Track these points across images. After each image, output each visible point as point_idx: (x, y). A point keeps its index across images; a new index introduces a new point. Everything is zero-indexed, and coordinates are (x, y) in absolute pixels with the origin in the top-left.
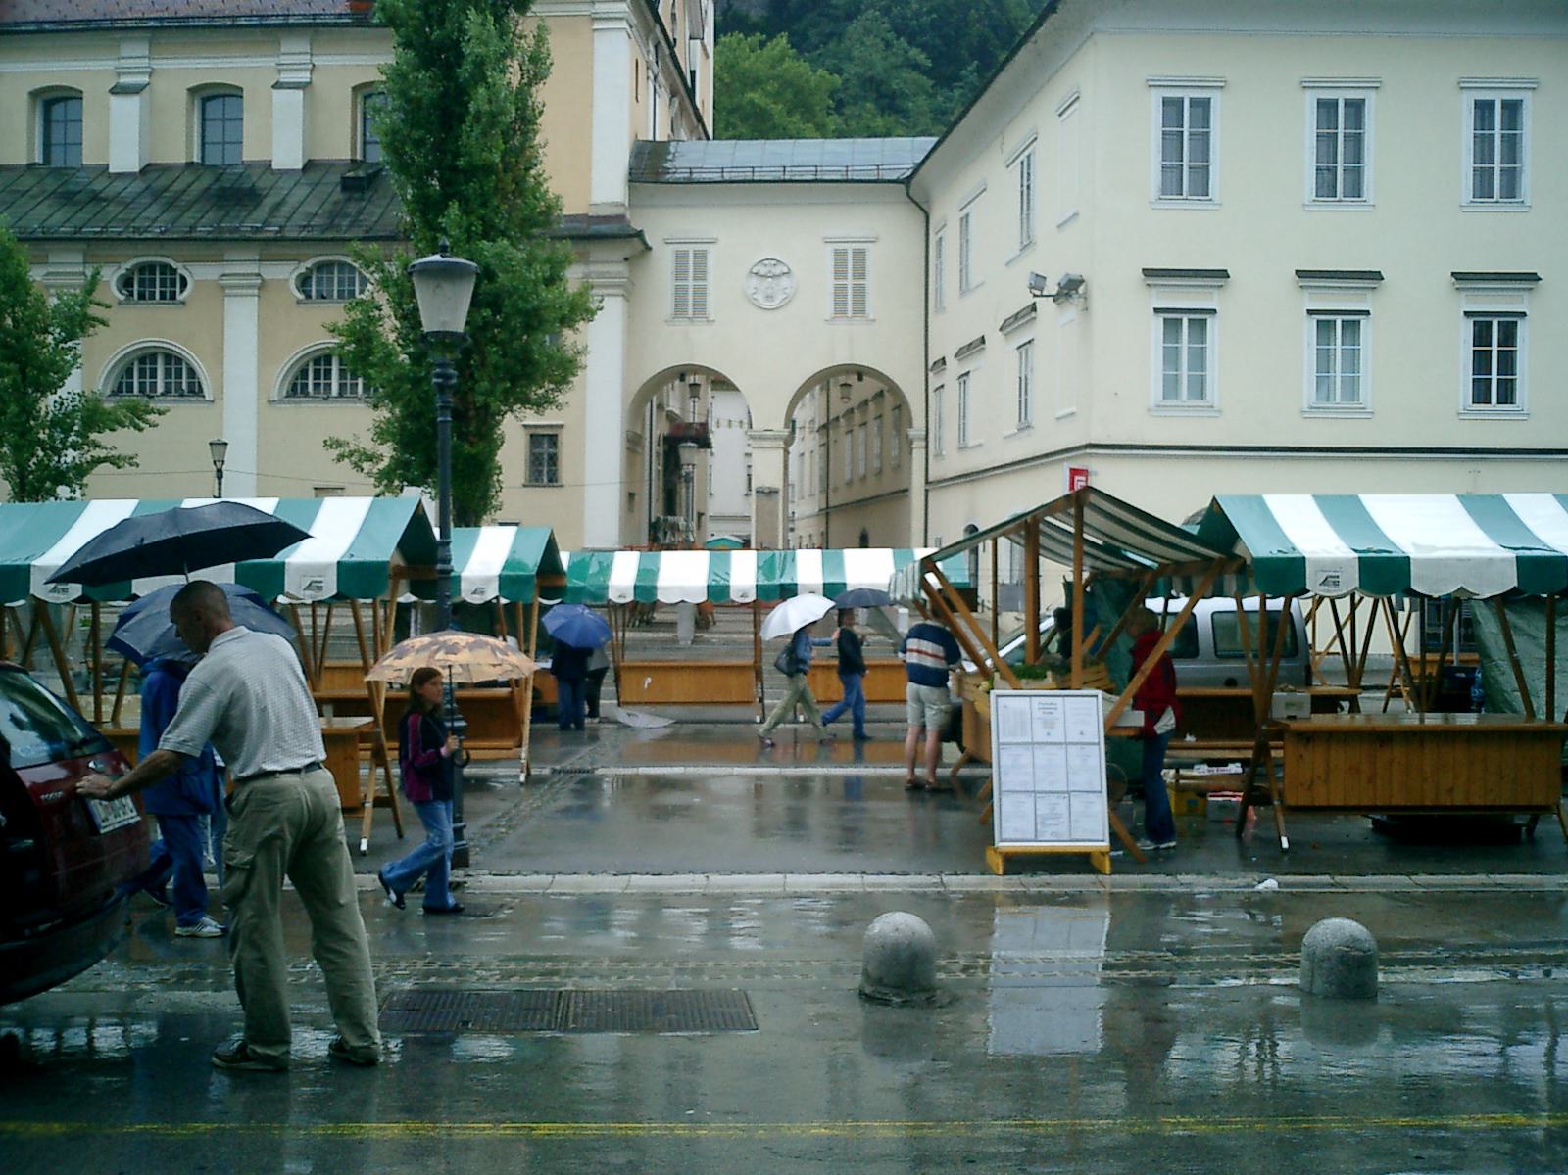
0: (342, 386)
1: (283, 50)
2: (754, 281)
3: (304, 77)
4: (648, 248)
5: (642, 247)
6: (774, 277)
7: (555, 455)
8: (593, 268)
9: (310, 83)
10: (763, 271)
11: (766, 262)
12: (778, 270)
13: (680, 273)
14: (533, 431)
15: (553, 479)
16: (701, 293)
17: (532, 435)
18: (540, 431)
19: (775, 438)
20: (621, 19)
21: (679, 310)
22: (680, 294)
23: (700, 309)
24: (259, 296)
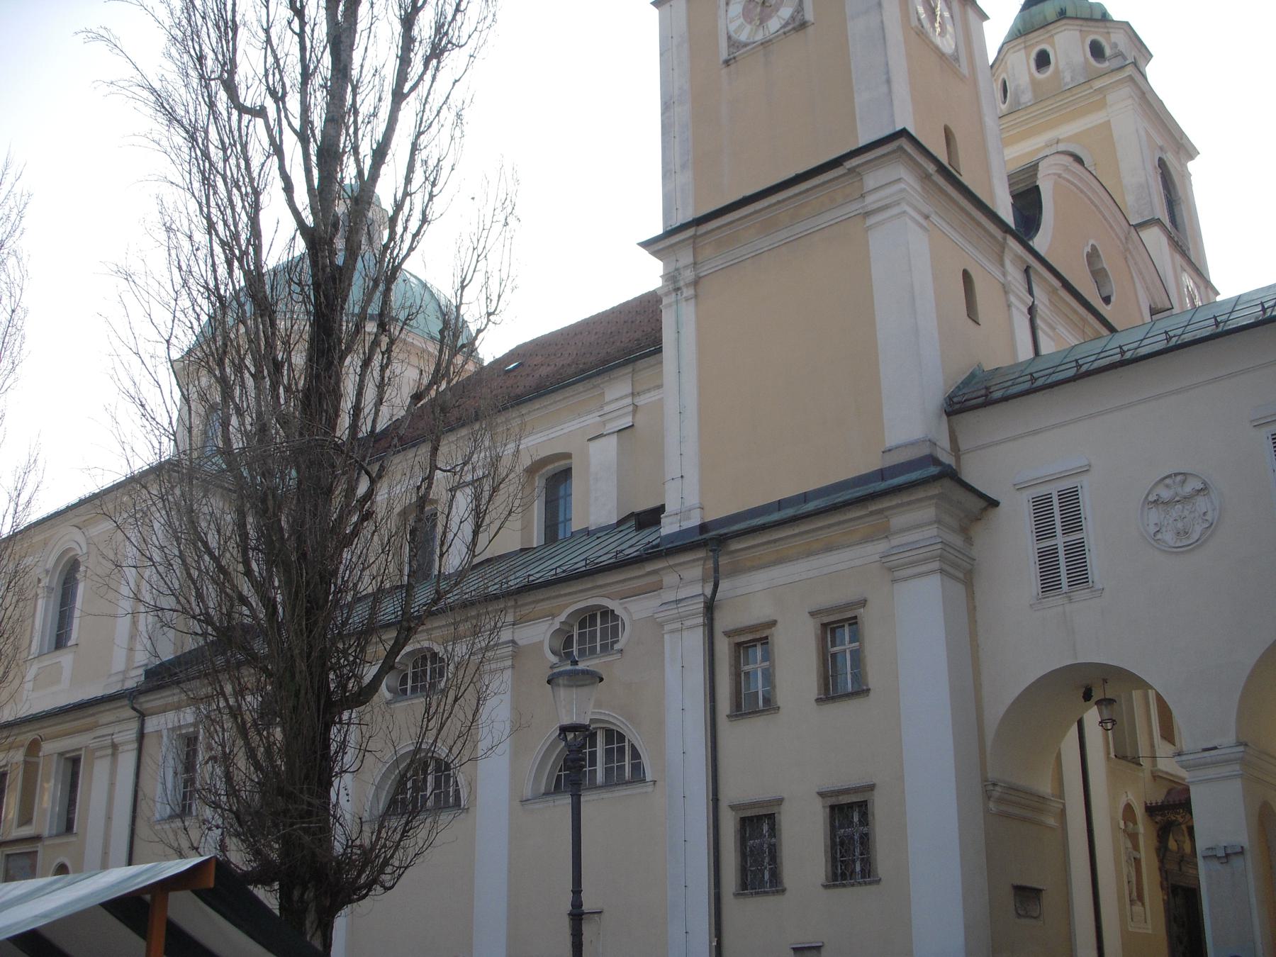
0: (608, 772)
1: (608, 398)
2: (1154, 516)
3: (627, 421)
4: (994, 504)
5: (975, 504)
6: (1187, 498)
7: (866, 835)
8: (896, 541)
9: (633, 425)
10: (1166, 494)
11: (1168, 481)
12: (1188, 489)
13: (1043, 530)
14: (833, 801)
15: (868, 874)
16: (1077, 552)
17: (832, 808)
18: (845, 800)
19: (1227, 762)
20: (897, 203)
21: (1049, 583)
22: (1047, 559)
23: (1080, 576)
24: (513, 667)
